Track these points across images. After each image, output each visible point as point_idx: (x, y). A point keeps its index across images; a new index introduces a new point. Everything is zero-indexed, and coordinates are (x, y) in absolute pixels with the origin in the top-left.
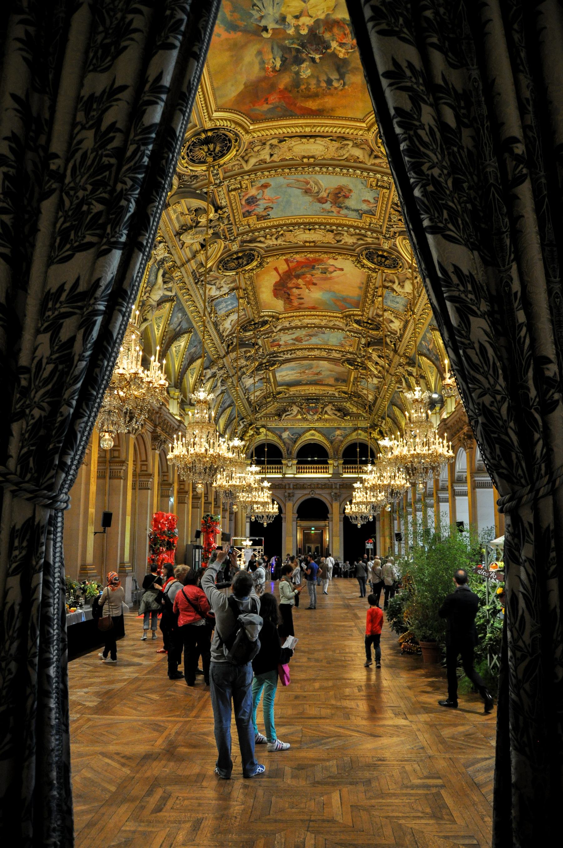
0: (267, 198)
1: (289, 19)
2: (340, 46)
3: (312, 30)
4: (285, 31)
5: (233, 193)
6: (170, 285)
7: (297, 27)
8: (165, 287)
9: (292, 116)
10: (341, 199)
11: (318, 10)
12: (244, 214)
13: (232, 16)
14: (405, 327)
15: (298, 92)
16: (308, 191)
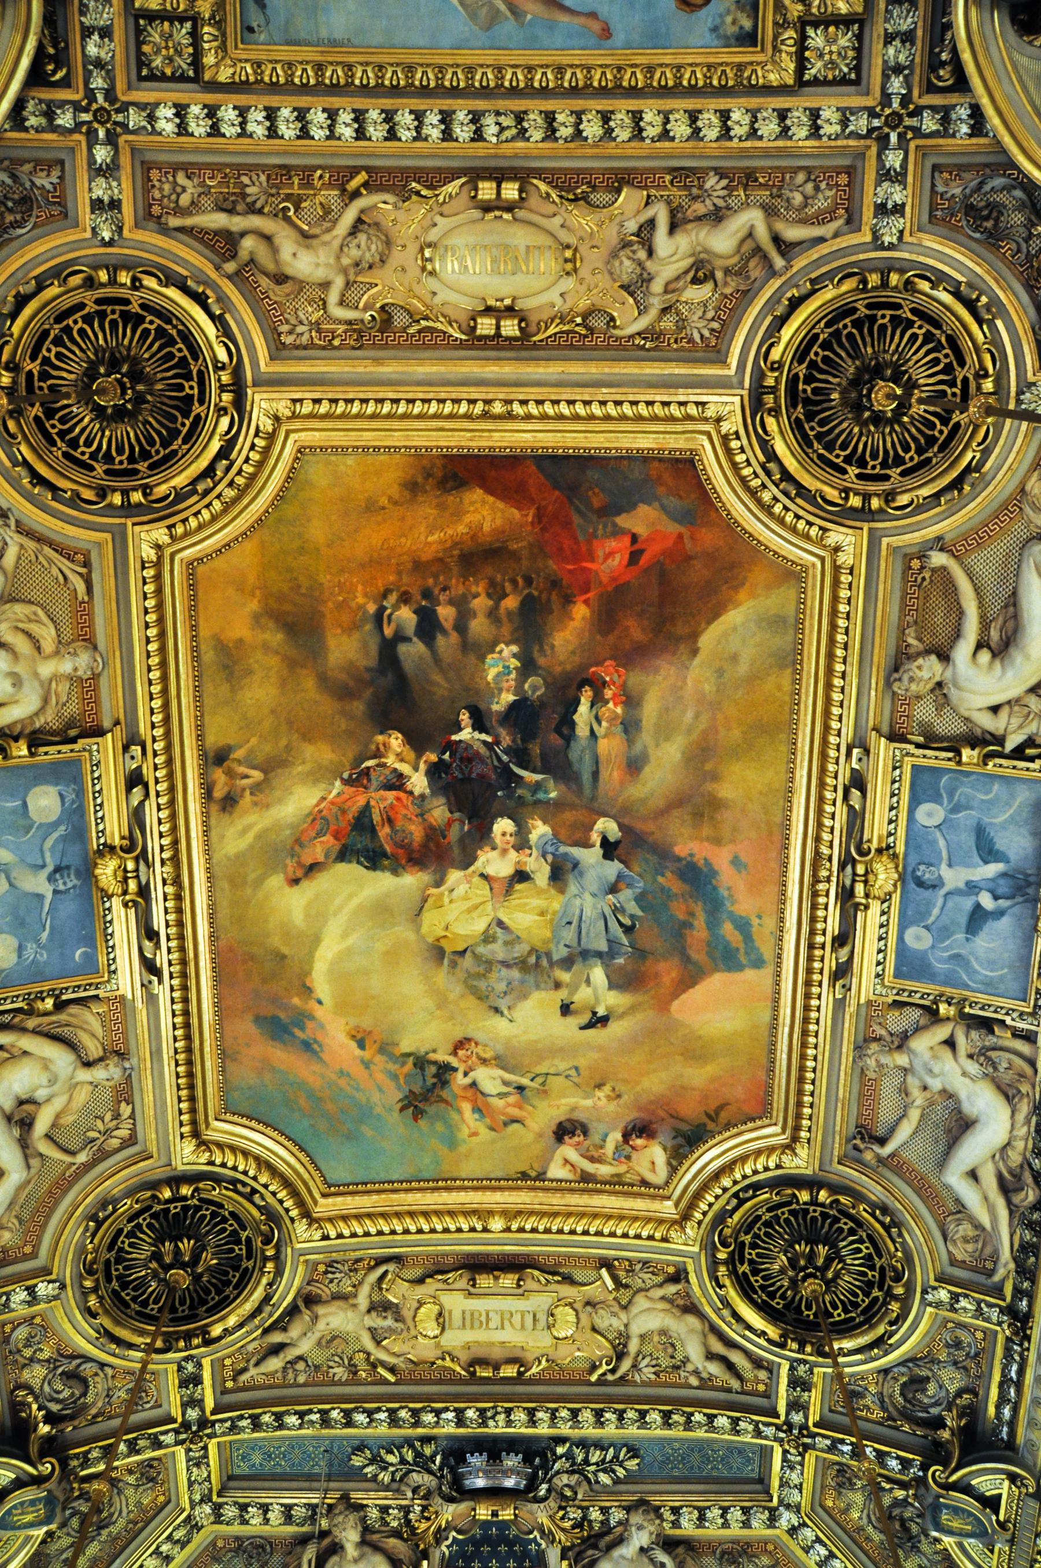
1: (541, 872)
2: (401, 776)
3: (482, 835)
4: (555, 834)
7: (522, 844)
9: (554, 458)
11: (466, 898)
13: (692, 914)
15: (529, 581)
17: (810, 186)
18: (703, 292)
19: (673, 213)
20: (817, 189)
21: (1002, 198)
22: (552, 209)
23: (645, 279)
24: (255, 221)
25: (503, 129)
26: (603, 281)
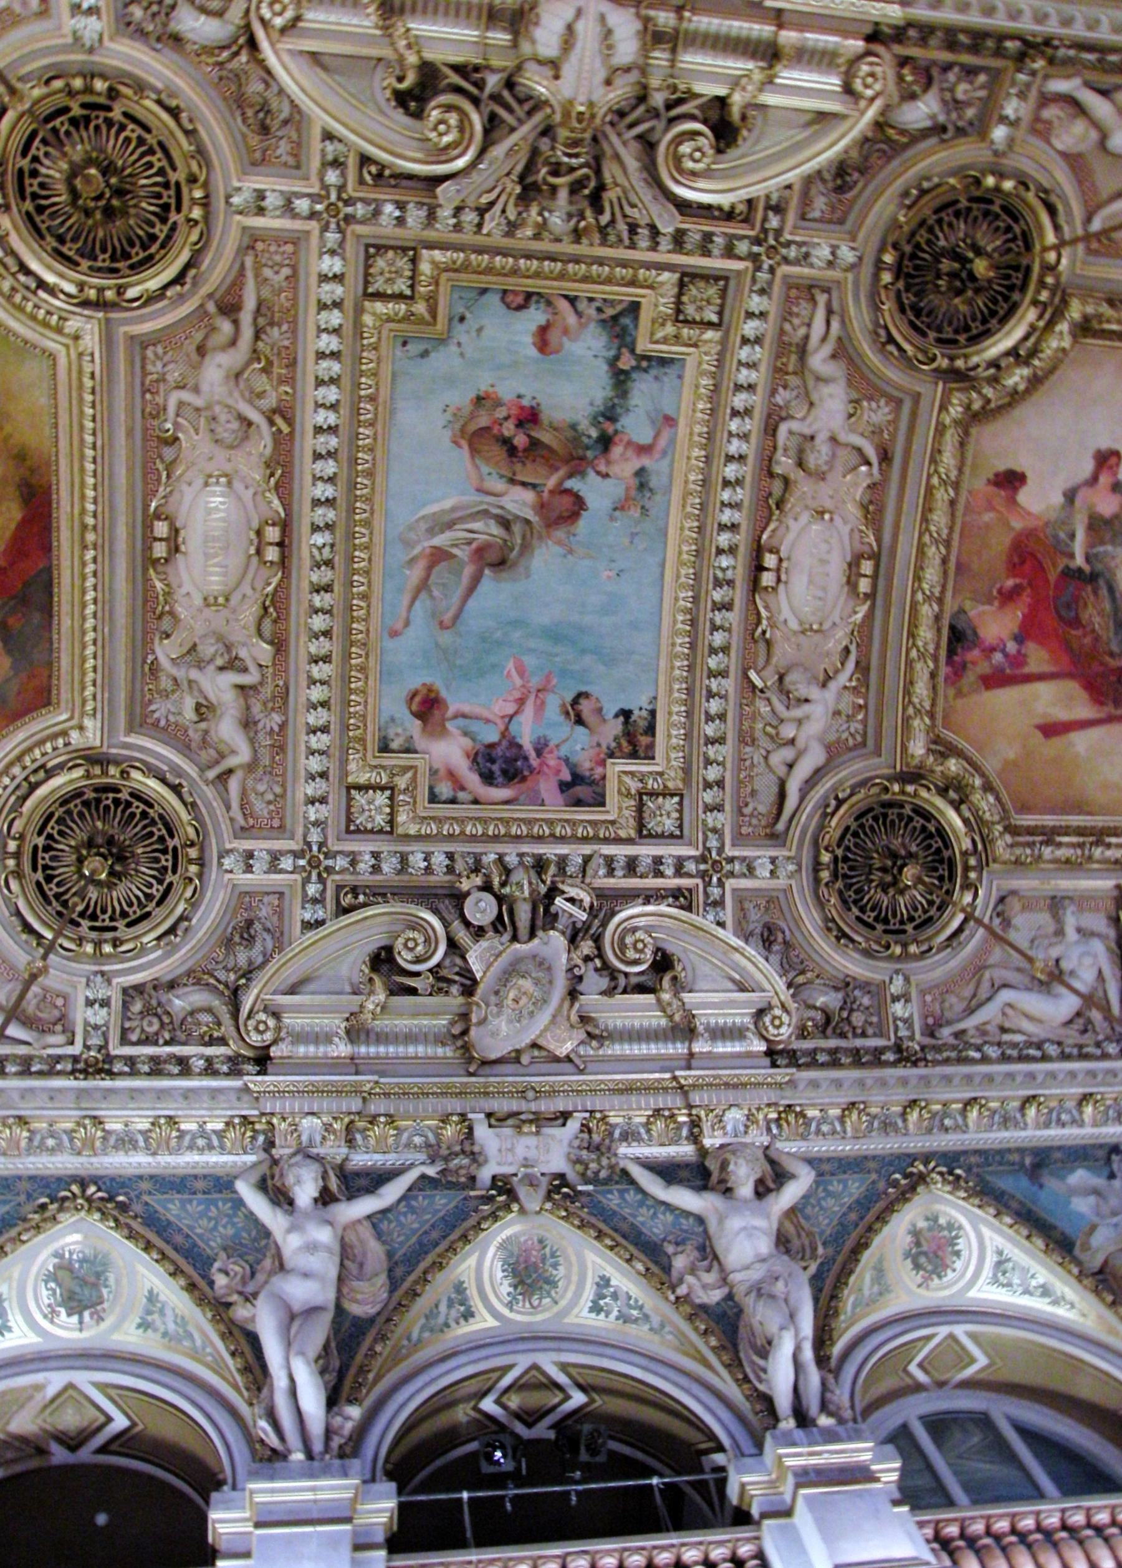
0: (510, 709)
5: (402, 818)
8: (746, 1190)
10: (545, 437)
12: (579, 803)
16: (492, 556)
17: (270, 797)
18: (190, 714)
19: (253, 687)
20: (269, 803)
21: (258, 947)
22: (259, 586)
23: (200, 665)
24: (247, 332)
25: (320, 549)
26: (200, 628)
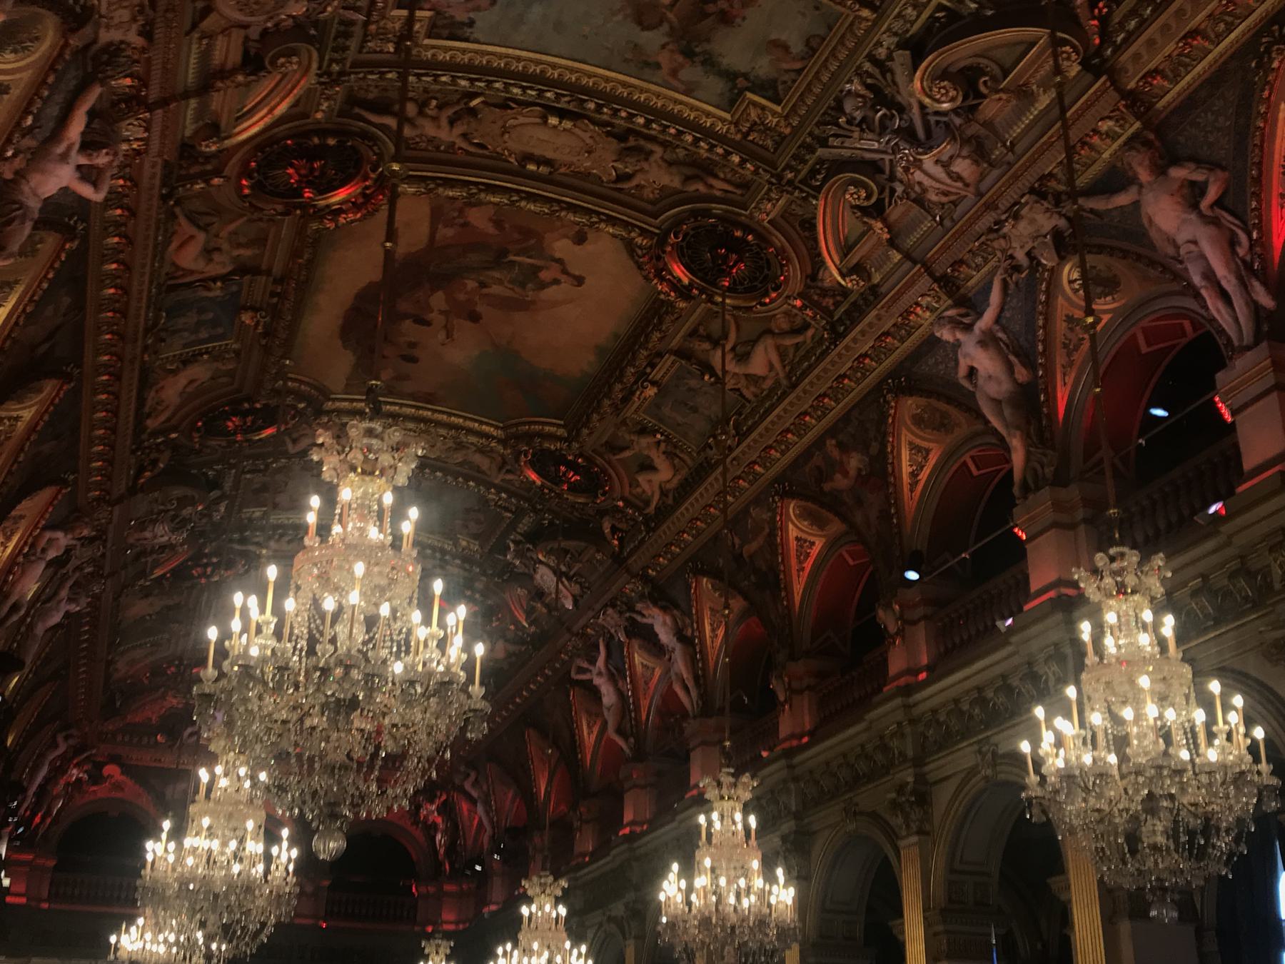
6: (102, 159)
14: (686, 488)
